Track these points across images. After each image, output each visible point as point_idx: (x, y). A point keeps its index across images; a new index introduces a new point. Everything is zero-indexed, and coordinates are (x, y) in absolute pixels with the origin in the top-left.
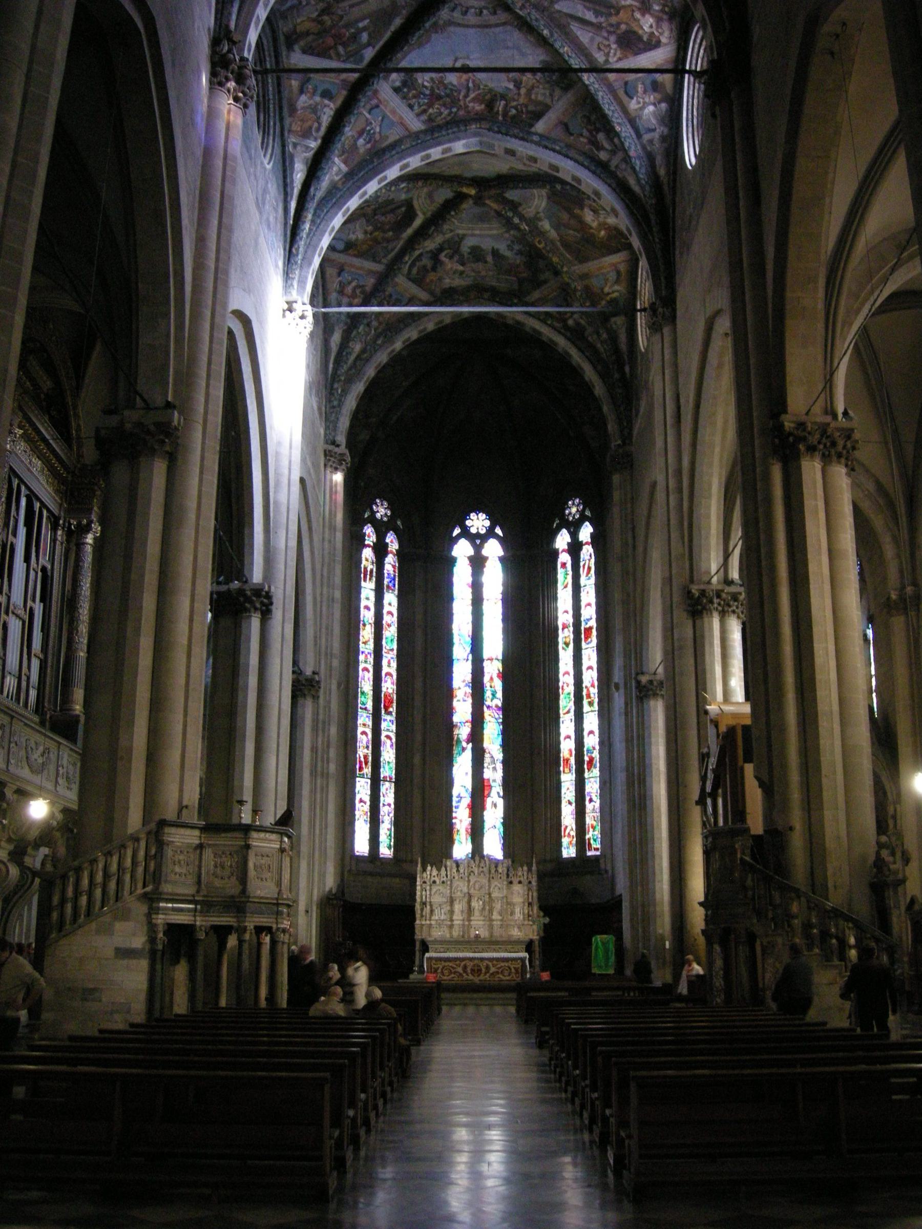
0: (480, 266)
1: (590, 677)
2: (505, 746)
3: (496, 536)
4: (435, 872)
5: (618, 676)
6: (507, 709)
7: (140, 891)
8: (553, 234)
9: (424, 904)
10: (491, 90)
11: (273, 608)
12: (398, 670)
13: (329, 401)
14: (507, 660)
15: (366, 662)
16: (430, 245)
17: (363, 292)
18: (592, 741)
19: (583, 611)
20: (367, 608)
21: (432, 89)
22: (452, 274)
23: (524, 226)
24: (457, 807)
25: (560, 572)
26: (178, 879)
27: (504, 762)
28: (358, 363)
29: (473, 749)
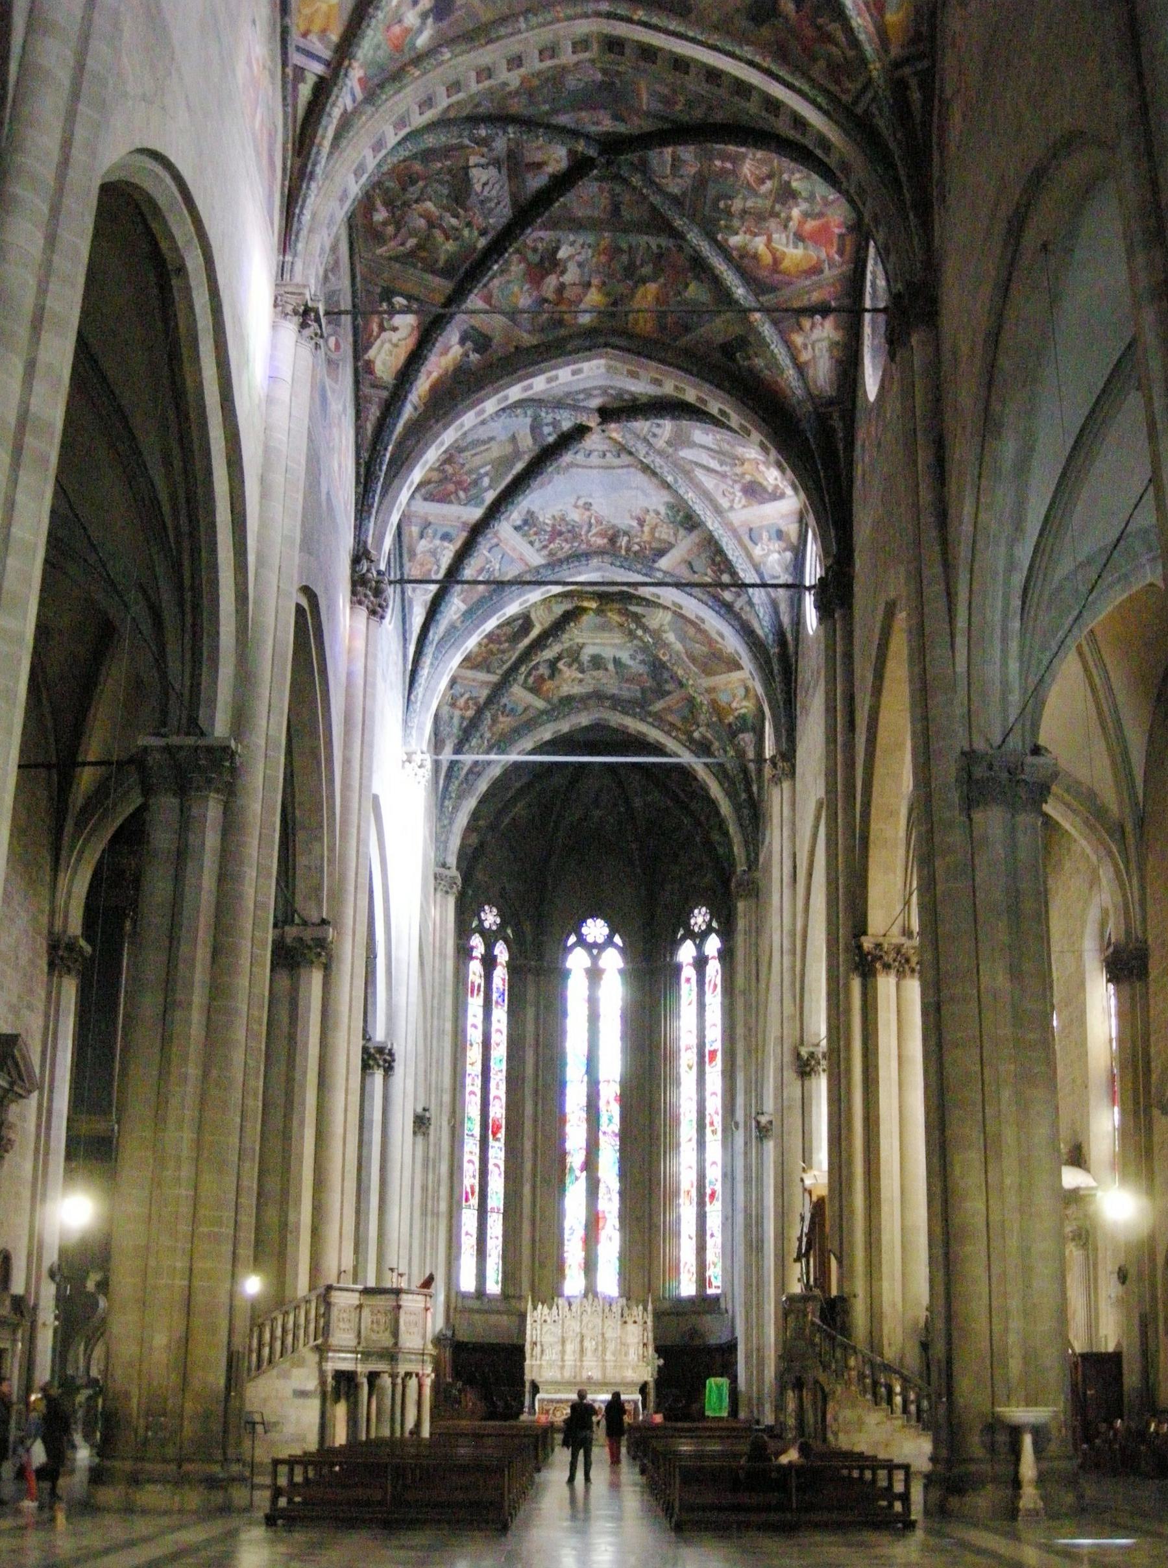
0: (601, 673)
1: (714, 1104)
2: (623, 1175)
3: (616, 946)
4: (546, 1311)
5: (740, 1115)
6: (626, 1136)
7: (312, 1343)
8: (678, 646)
10: (614, 526)
11: (395, 1064)
12: (508, 1092)
13: (439, 819)
14: (625, 1084)
16: (548, 654)
17: (475, 704)
18: (714, 1174)
19: (707, 1032)
20: (474, 1026)
21: (554, 526)
22: (570, 682)
23: (648, 638)
25: (684, 987)
26: (342, 1336)
28: (470, 777)
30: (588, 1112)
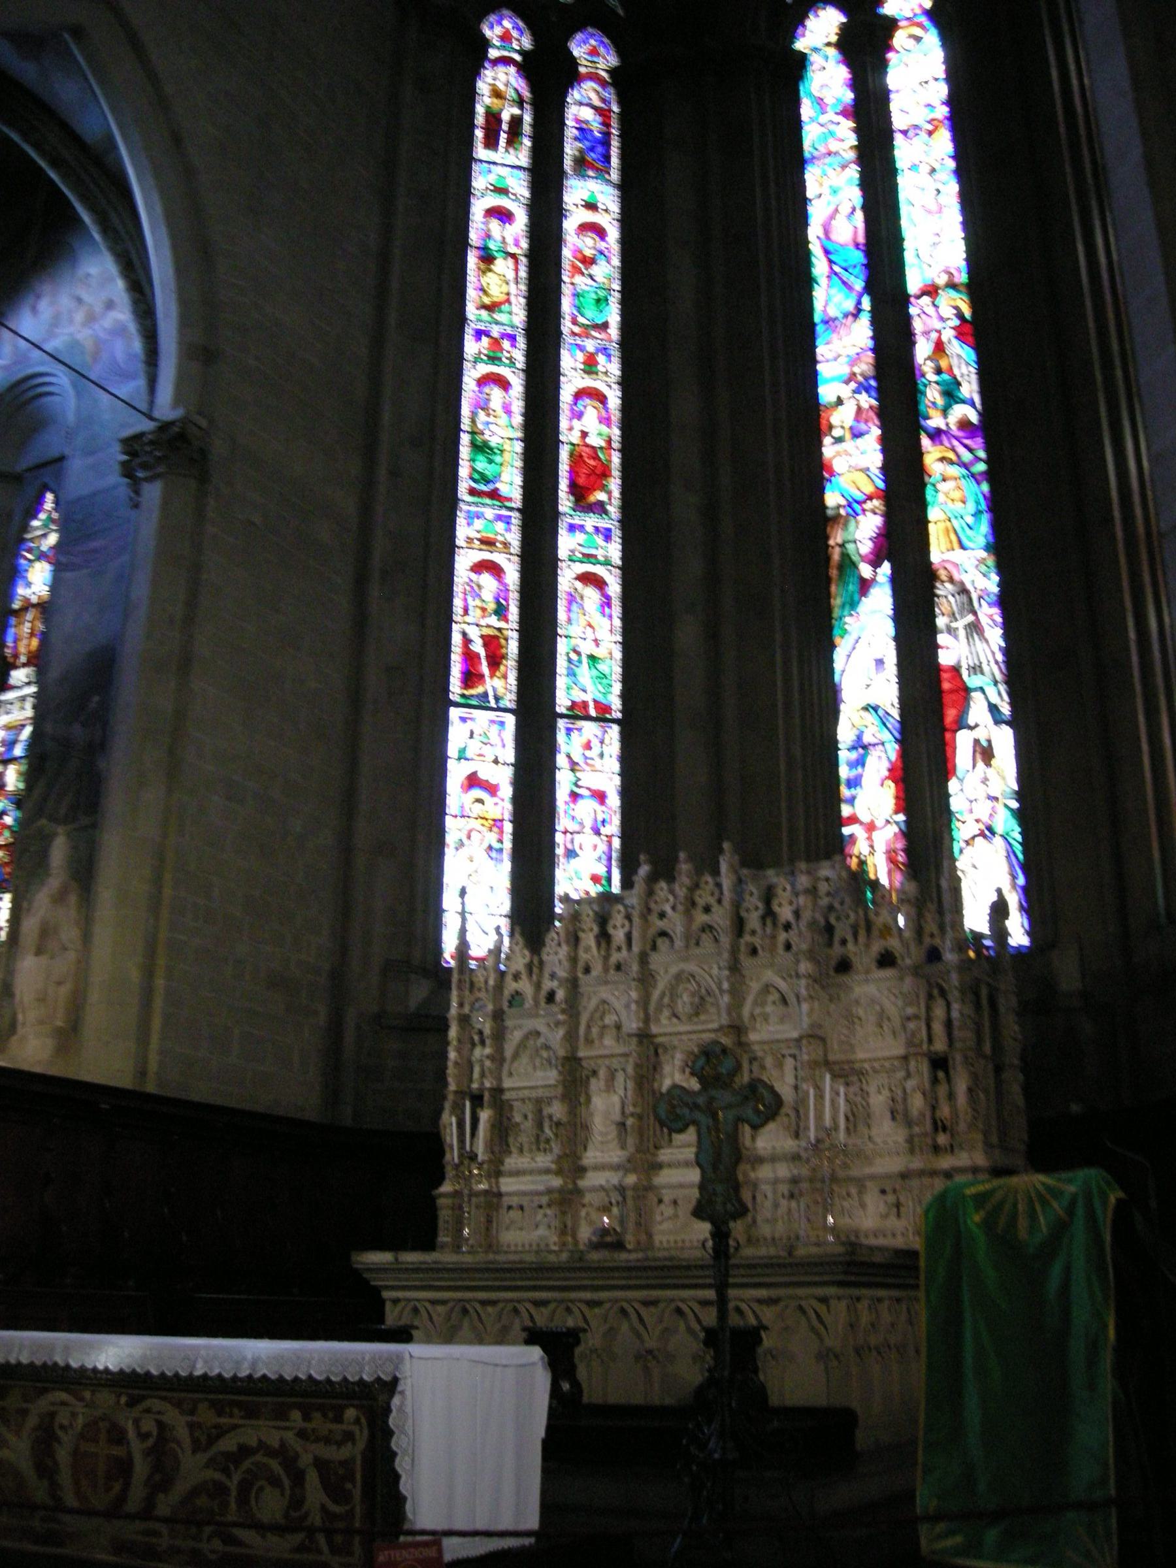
2: (1005, 549)
12: (625, 383)
15: (493, 359)
24: (854, 783)
27: (1004, 601)
29: (894, 580)
30: (881, 394)
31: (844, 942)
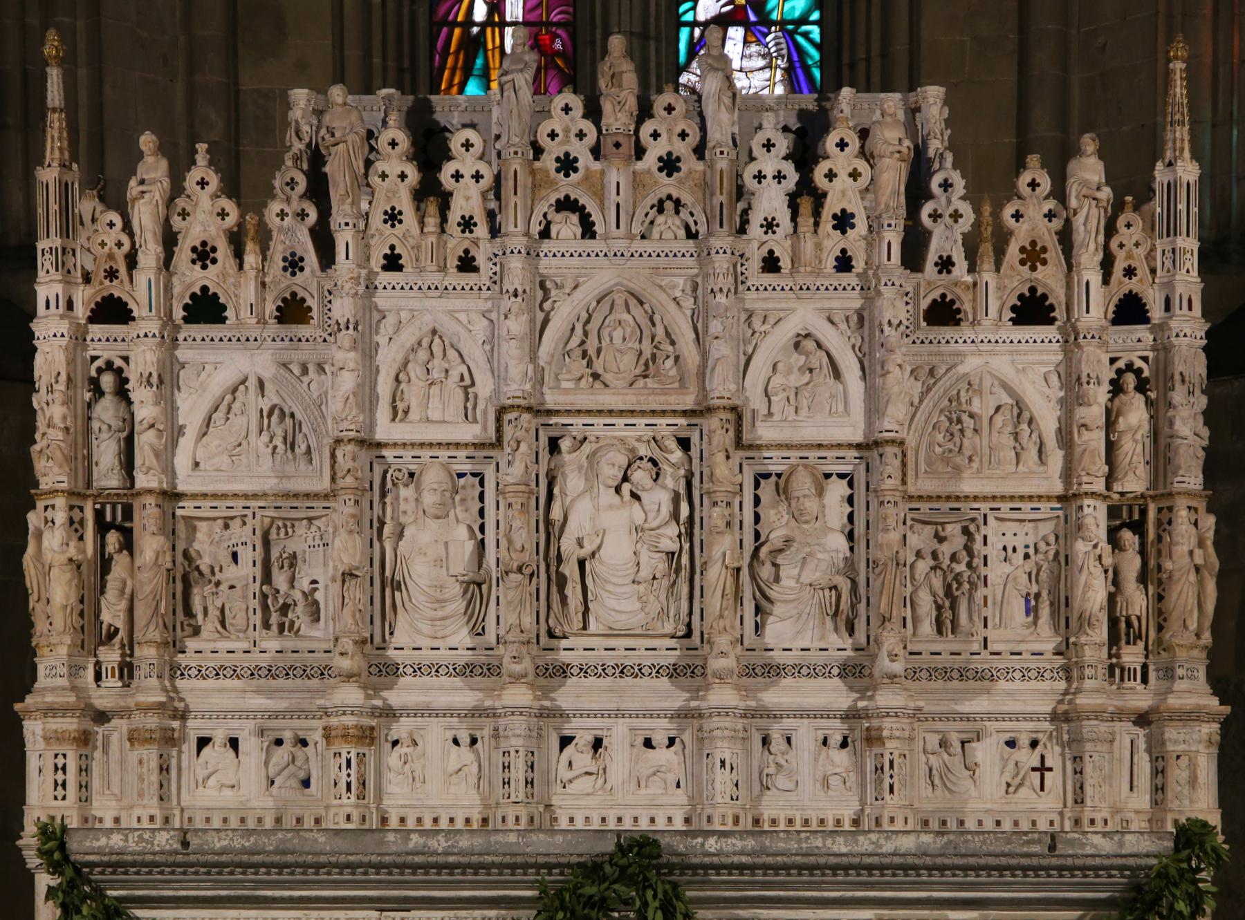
4: (207, 216)
9: (114, 522)
31: (946, 264)
